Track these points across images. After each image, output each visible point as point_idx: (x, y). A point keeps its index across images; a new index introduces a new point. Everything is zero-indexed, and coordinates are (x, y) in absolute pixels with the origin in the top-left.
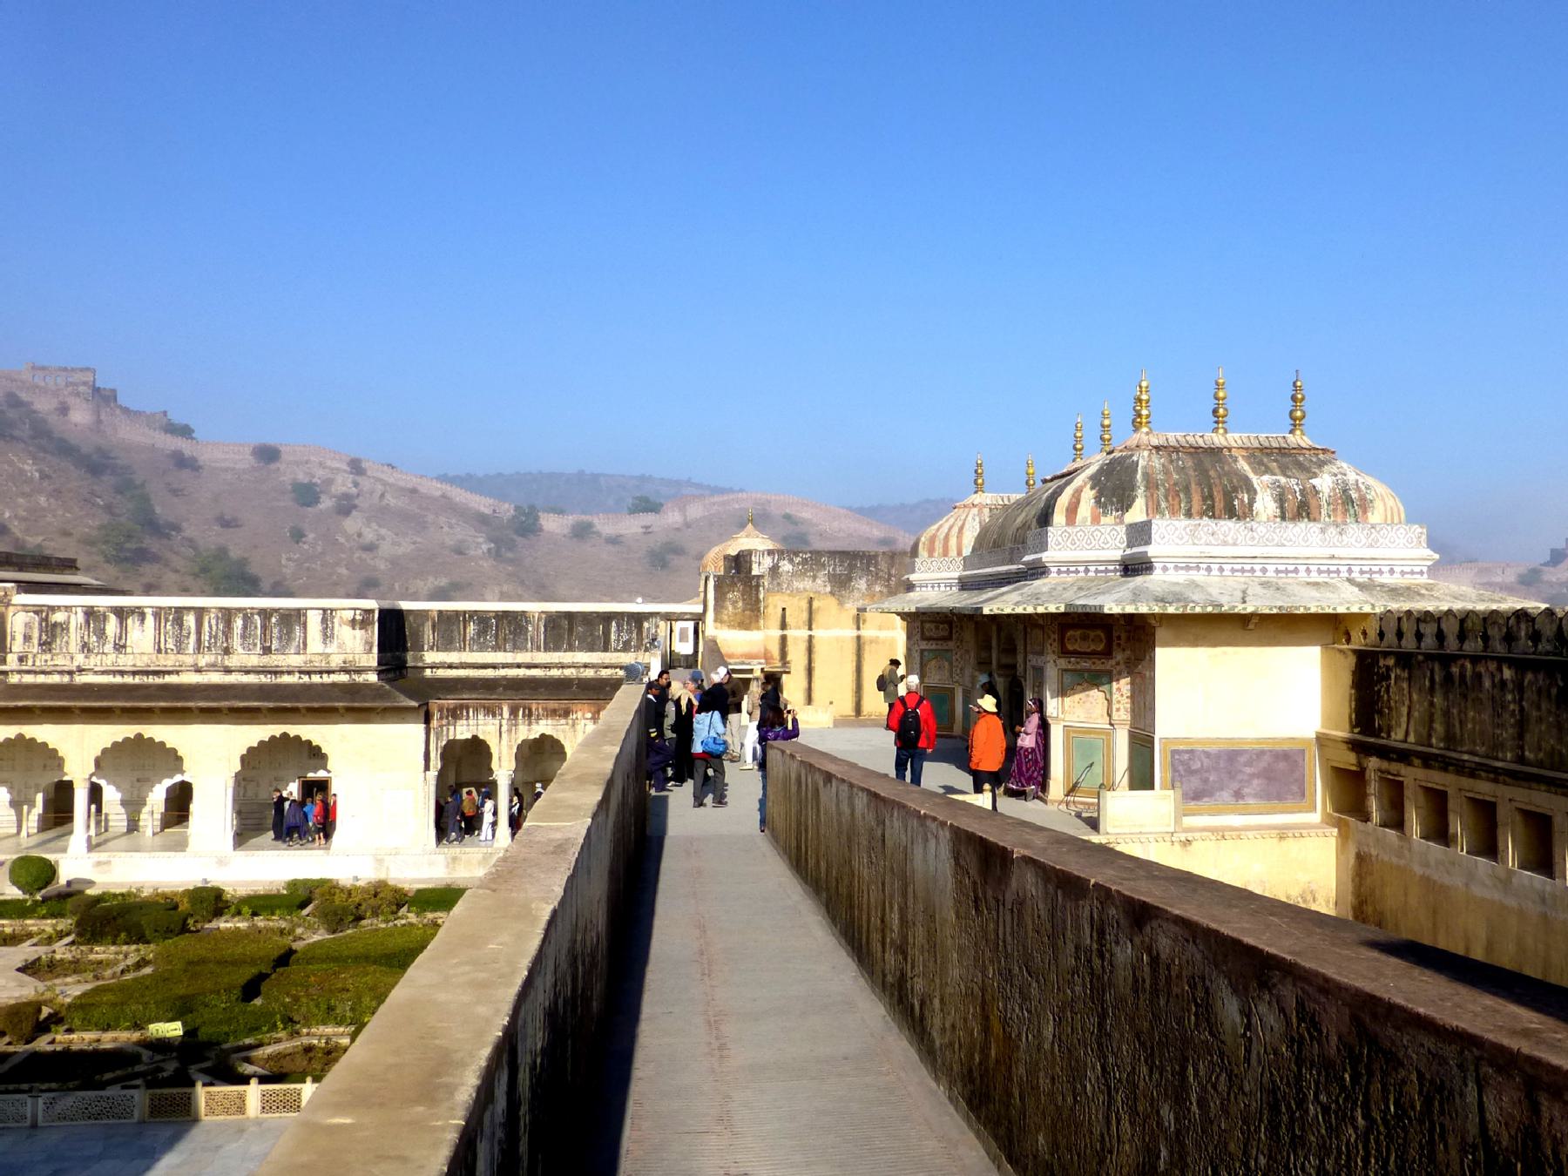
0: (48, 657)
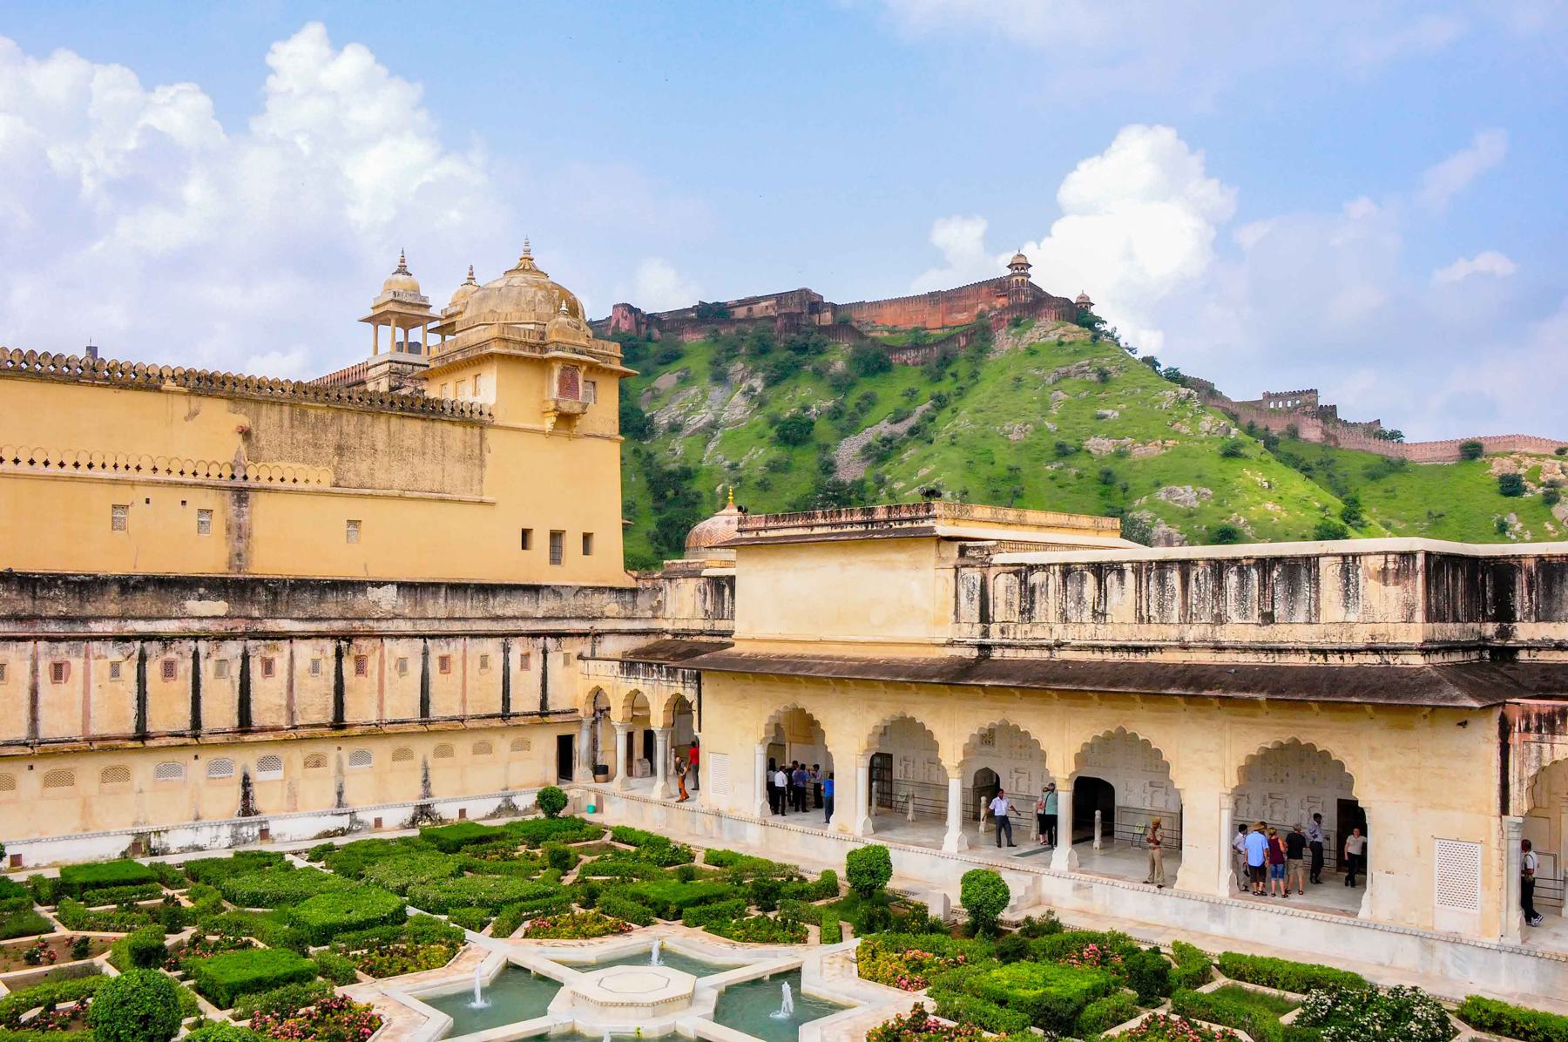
0: (1027, 627)
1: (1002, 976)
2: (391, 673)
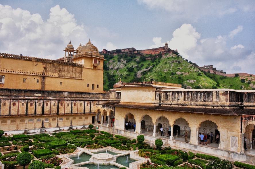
1: (162, 156)
2: (66, 106)
